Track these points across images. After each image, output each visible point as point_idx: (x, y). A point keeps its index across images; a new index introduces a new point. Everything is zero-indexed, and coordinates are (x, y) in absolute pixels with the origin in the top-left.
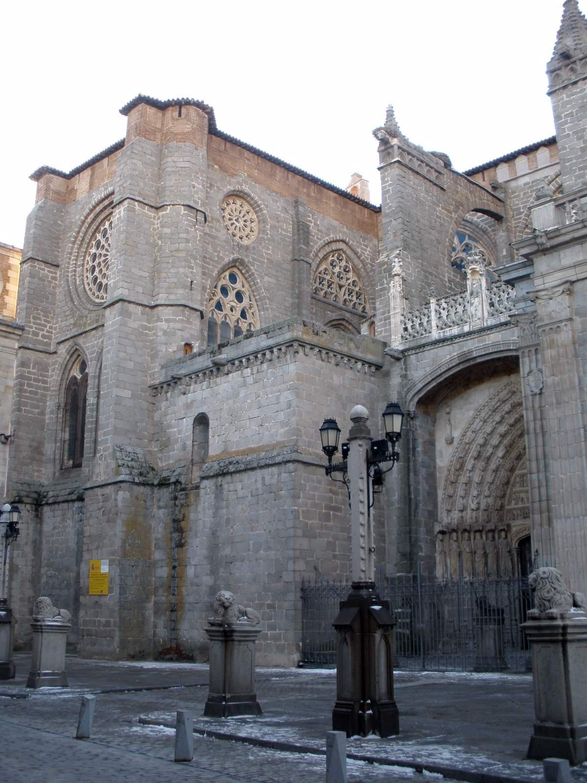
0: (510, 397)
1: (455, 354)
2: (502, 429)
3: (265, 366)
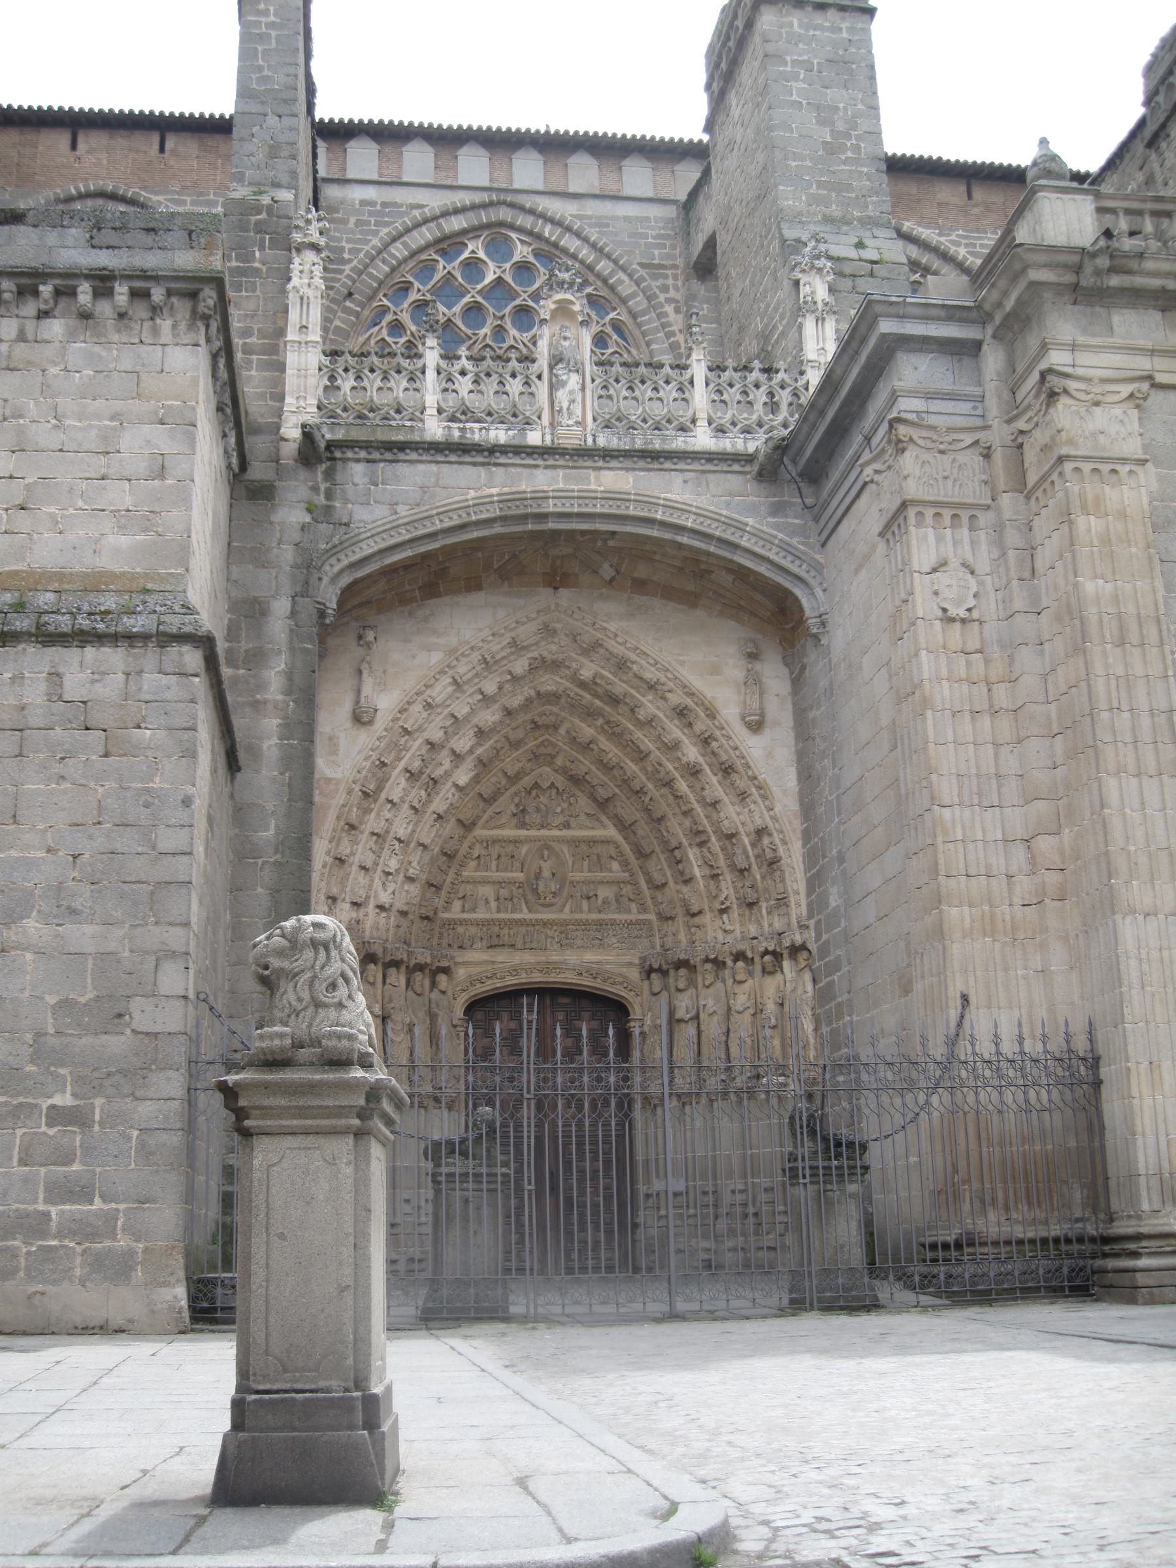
0: (536, 644)
1: (494, 491)
2: (489, 717)
3: (56, 328)
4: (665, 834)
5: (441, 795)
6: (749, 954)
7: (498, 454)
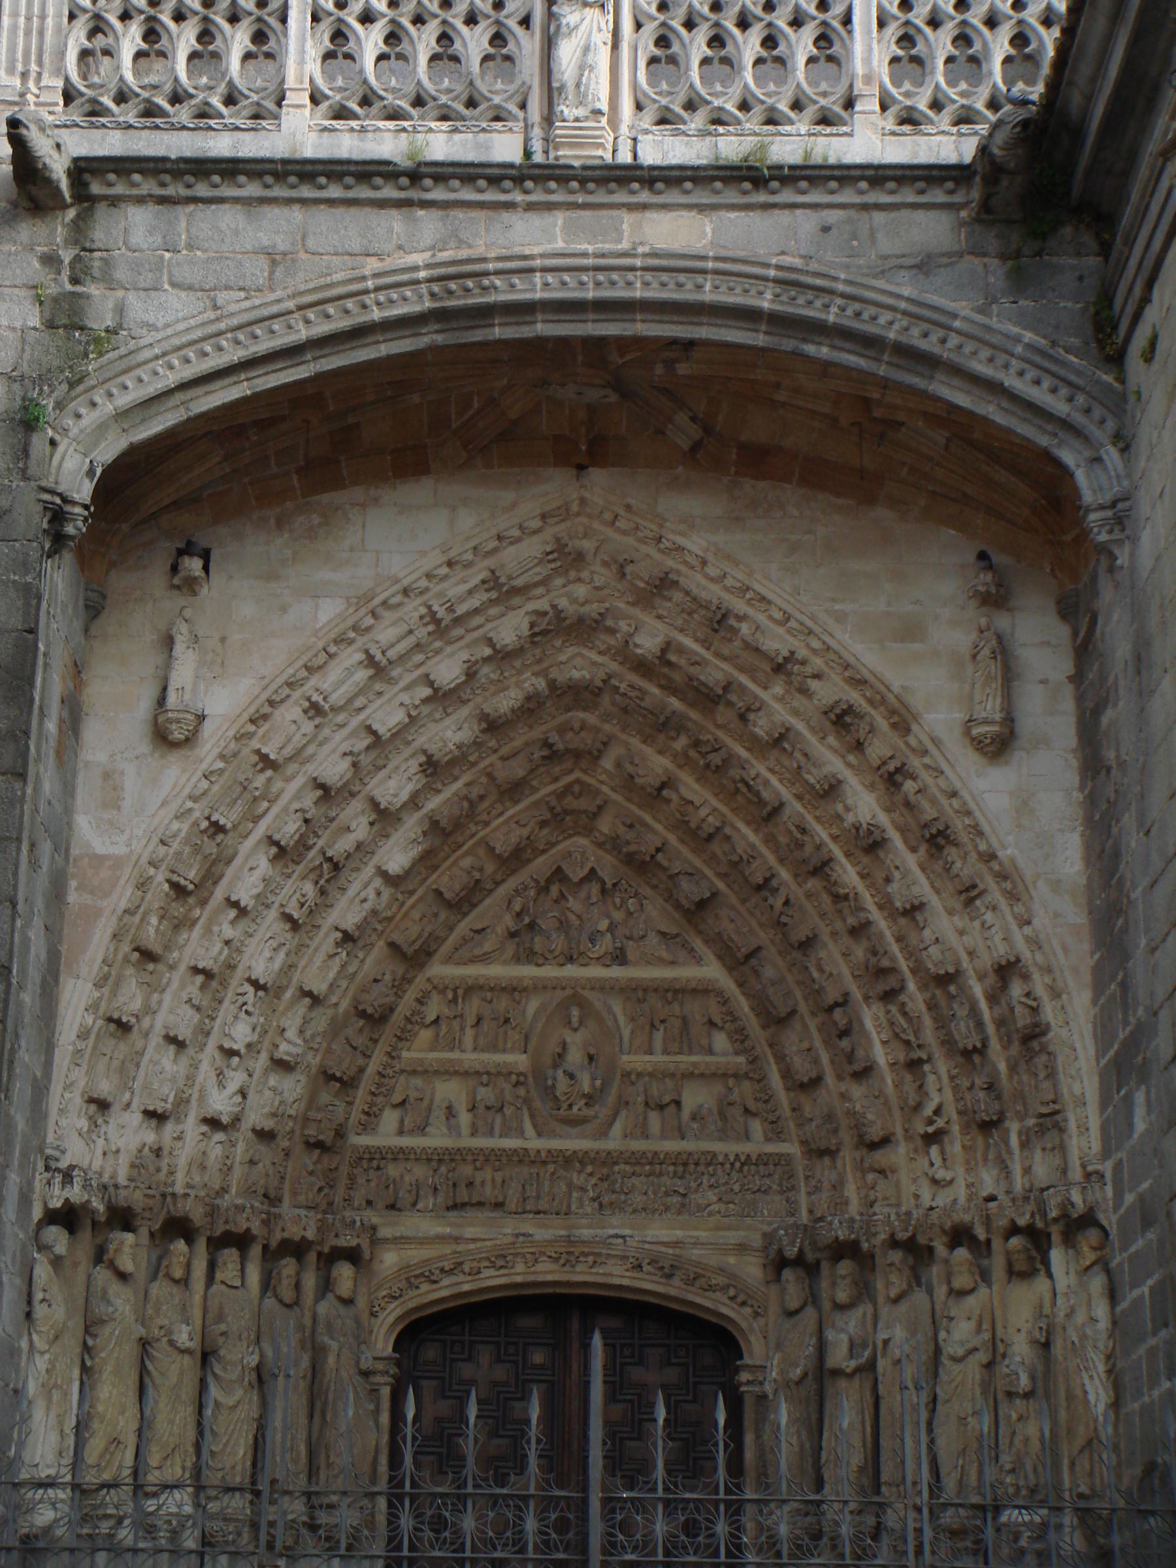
0: (544, 582)
4: (815, 975)
5: (351, 892)
6: (981, 1233)
7: (428, 182)
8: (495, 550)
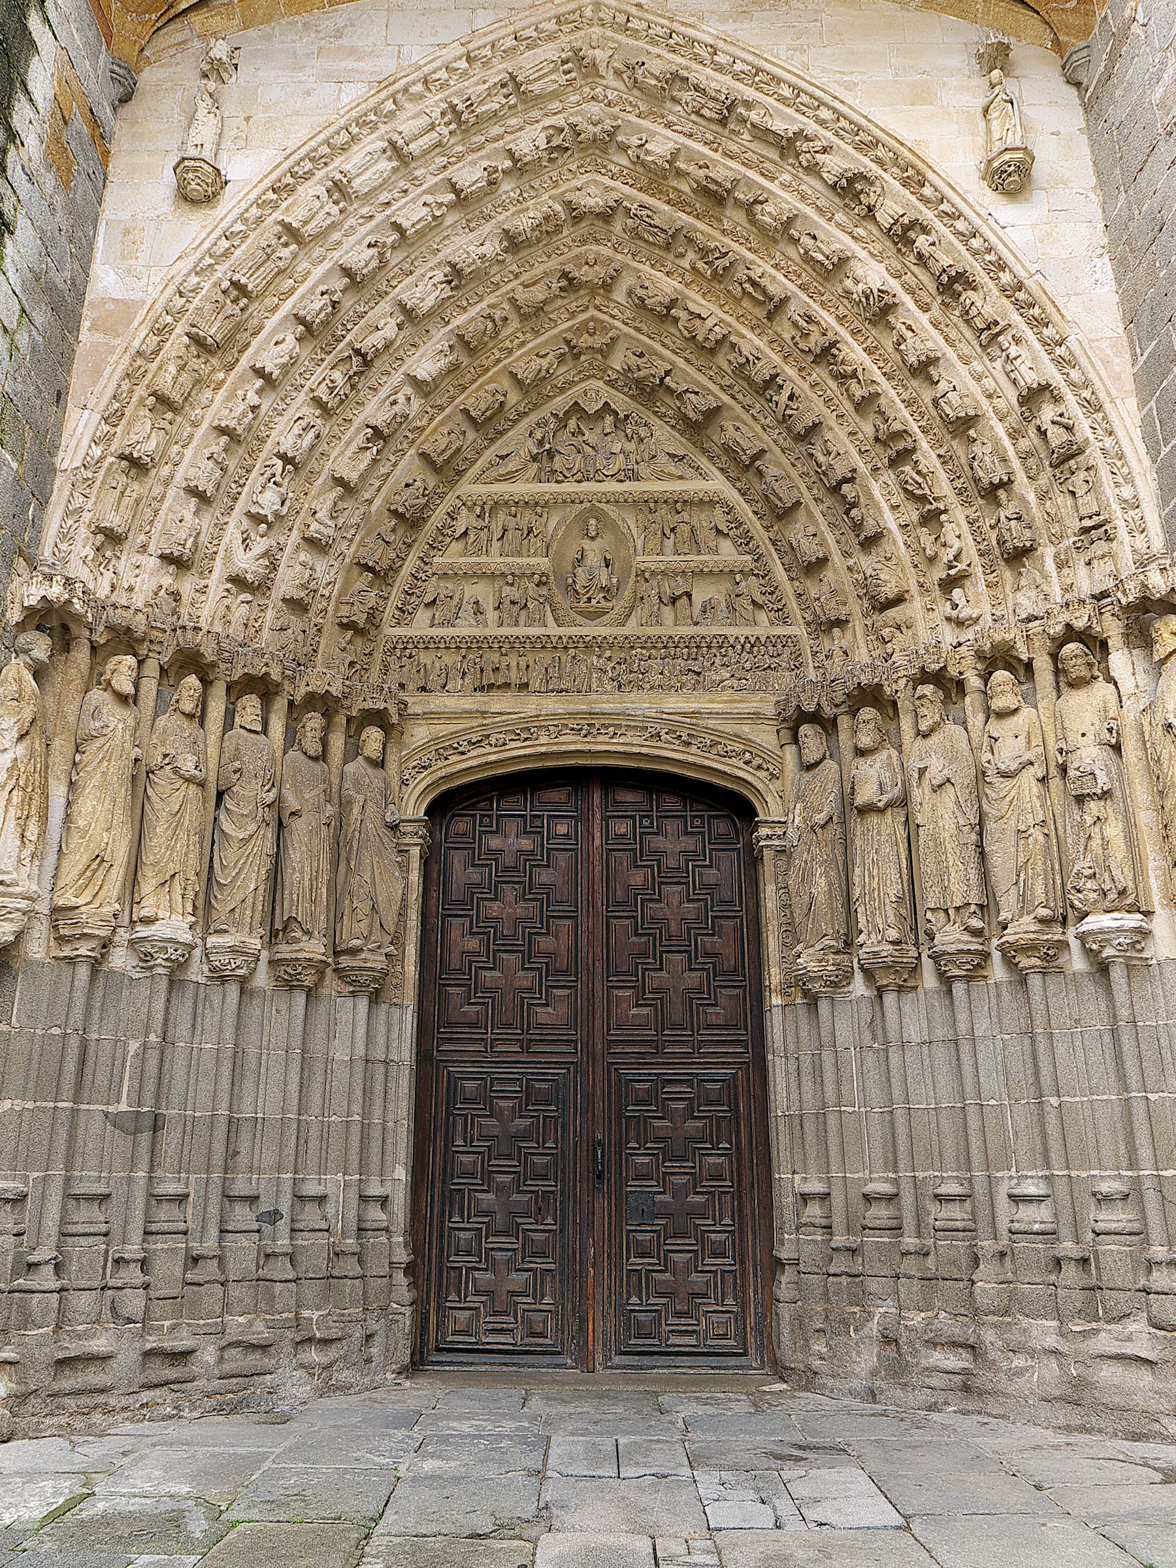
4: (822, 459)
5: (383, 393)
8: (509, 53)
